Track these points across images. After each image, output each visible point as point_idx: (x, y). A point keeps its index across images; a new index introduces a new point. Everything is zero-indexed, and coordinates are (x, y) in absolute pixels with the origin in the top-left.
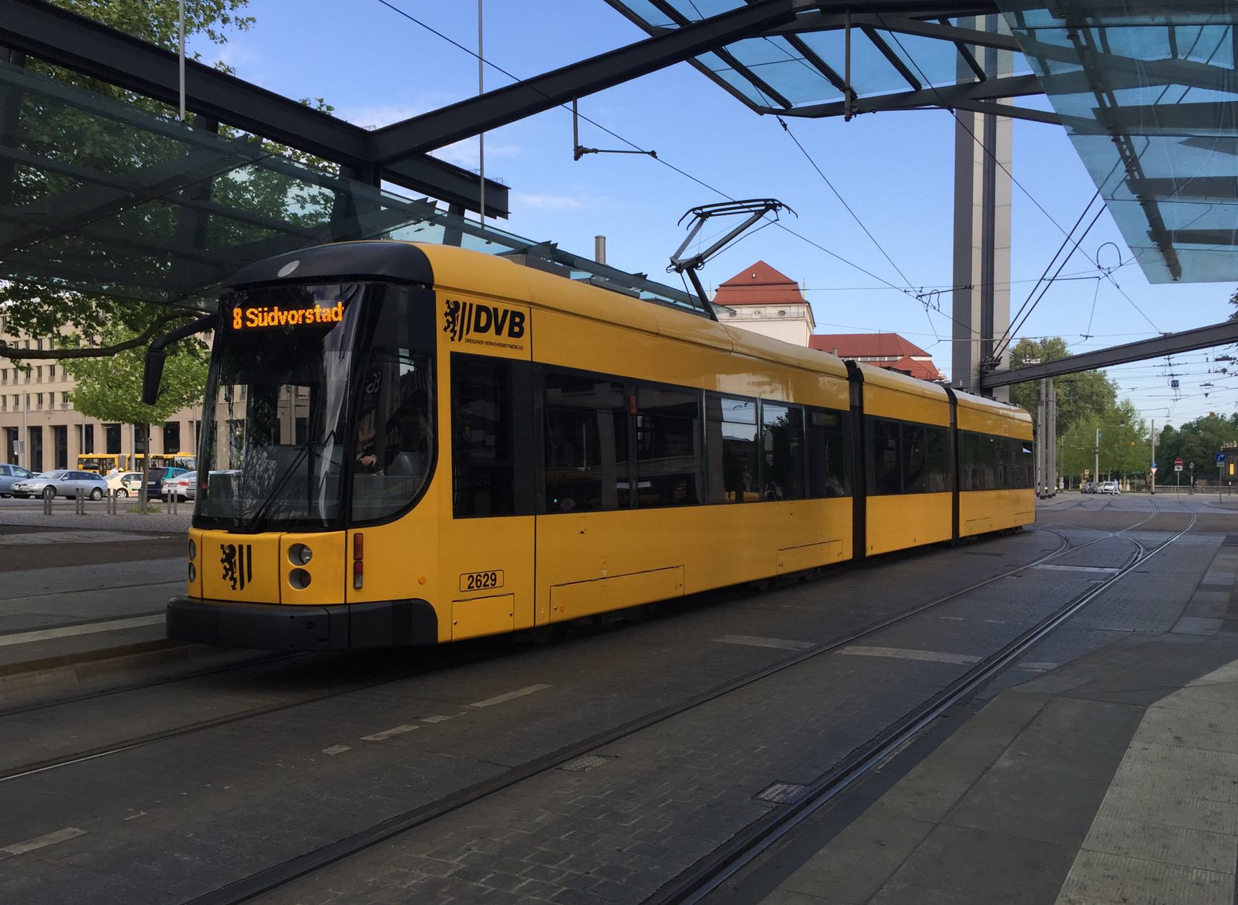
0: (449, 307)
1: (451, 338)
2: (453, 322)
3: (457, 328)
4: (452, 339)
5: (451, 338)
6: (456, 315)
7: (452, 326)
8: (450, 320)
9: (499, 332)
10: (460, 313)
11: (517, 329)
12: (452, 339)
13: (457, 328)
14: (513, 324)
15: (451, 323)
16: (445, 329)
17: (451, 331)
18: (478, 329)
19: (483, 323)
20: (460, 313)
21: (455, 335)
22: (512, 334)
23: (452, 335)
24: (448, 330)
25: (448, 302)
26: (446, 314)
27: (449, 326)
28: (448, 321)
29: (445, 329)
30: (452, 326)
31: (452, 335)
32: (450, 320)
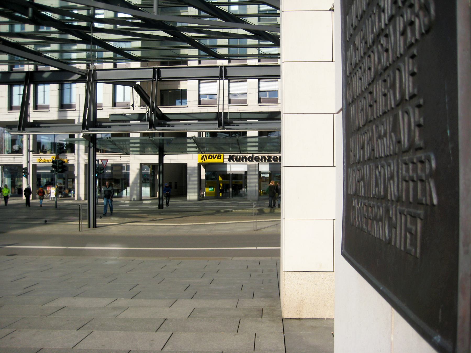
2: (203, 158)
3: (204, 159)
4: (203, 161)
9: (214, 158)
10: (205, 157)
11: (219, 158)
12: (203, 161)
13: (204, 159)
14: (218, 157)
16: (201, 160)
18: (209, 158)
19: (210, 157)
20: (205, 157)
22: (218, 158)
25: (202, 155)
26: (201, 157)
29: (201, 160)
32: (202, 158)
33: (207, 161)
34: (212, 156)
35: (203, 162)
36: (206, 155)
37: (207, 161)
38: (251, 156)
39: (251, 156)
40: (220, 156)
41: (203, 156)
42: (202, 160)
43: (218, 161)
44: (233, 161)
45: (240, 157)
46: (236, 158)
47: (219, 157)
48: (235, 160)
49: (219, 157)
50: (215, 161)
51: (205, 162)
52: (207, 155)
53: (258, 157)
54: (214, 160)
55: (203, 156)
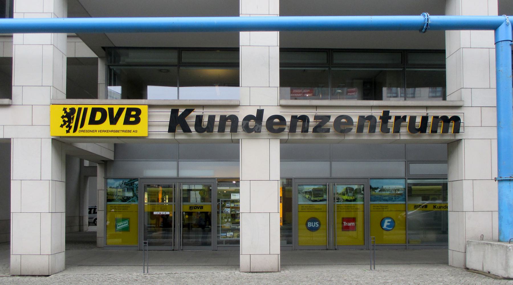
0: (66, 112)
1: (67, 131)
2: (70, 122)
3: (73, 125)
4: (68, 132)
5: (67, 131)
6: (72, 116)
7: (67, 124)
8: (66, 119)
12: (68, 132)
15: (67, 122)
16: (62, 126)
17: (67, 127)
21: (70, 129)
23: (68, 129)
24: (65, 127)
25: (65, 109)
26: (63, 117)
27: (65, 124)
28: (64, 121)
30: (67, 124)
31: (68, 129)
32: (66, 119)
33: (84, 131)
34: (103, 111)
35: (71, 134)
36: (80, 109)
37: (84, 131)
38: (255, 115)
39: (255, 115)
40: (133, 113)
41: (68, 111)
42: (65, 129)
43: (129, 131)
44: (186, 129)
45: (212, 118)
46: (199, 118)
47: (133, 116)
48: (193, 129)
49: (133, 116)
50: (117, 131)
51: (77, 134)
52: (86, 110)
53: (282, 119)
54: (113, 127)
55: (68, 111)
